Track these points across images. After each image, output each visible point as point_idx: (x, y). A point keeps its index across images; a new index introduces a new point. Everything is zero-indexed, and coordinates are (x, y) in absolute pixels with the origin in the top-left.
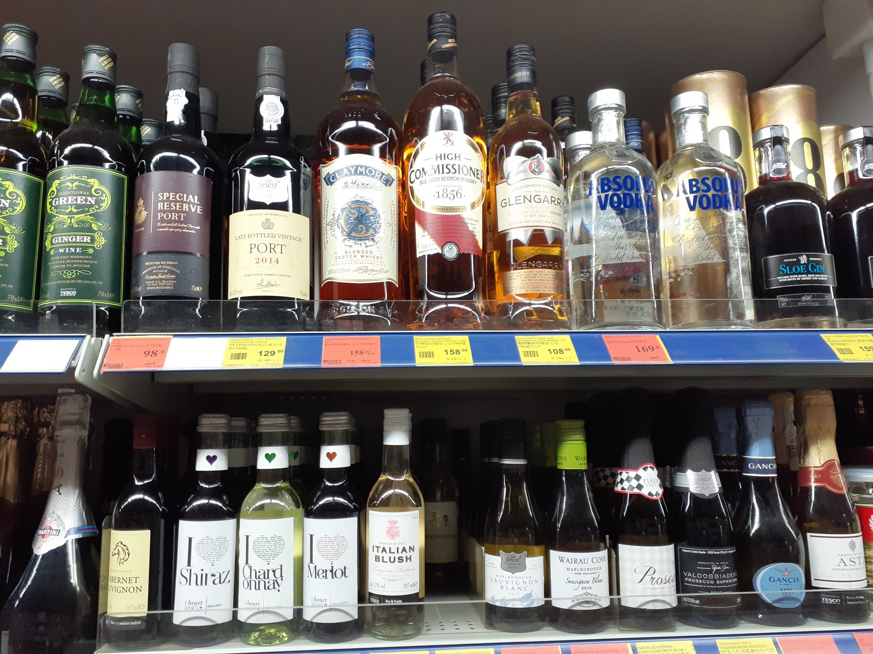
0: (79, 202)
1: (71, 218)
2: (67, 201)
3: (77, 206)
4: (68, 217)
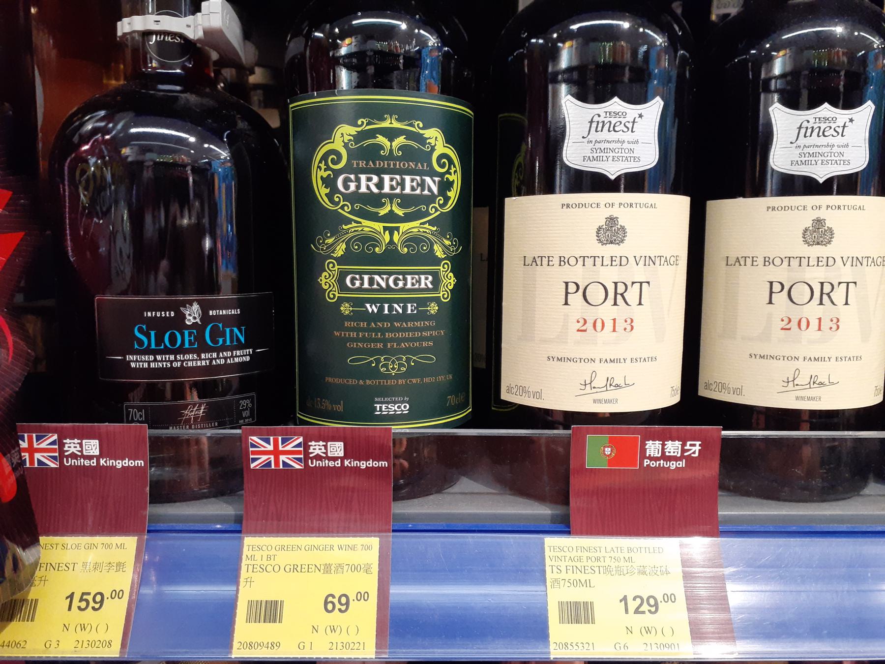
0: (408, 190)
1: (391, 231)
2: (380, 185)
3: (406, 201)
4: (385, 228)
